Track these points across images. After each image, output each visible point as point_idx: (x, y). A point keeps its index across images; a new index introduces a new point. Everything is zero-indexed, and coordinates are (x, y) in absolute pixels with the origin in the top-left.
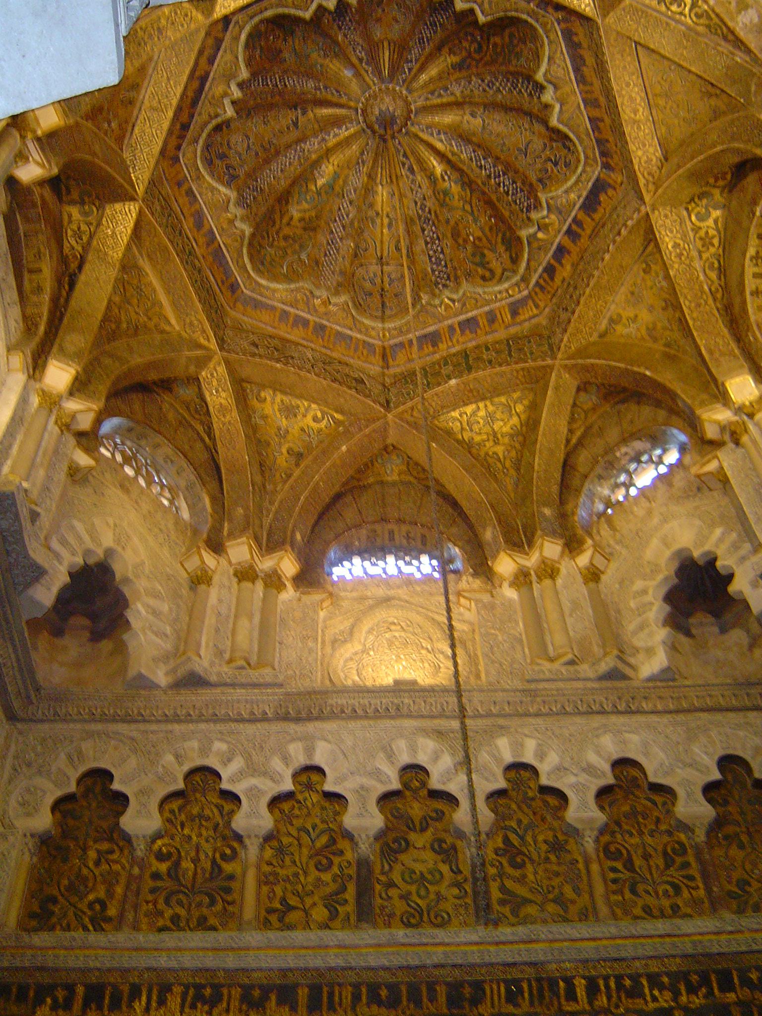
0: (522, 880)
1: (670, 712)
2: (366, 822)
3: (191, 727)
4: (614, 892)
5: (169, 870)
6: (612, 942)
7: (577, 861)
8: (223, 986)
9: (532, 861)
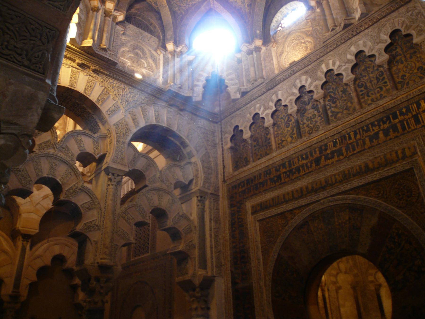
0: (336, 107)
1: (371, 26)
2: (293, 110)
3: (251, 104)
4: (362, 98)
5: (257, 143)
6: (359, 117)
7: (350, 93)
9: (338, 99)
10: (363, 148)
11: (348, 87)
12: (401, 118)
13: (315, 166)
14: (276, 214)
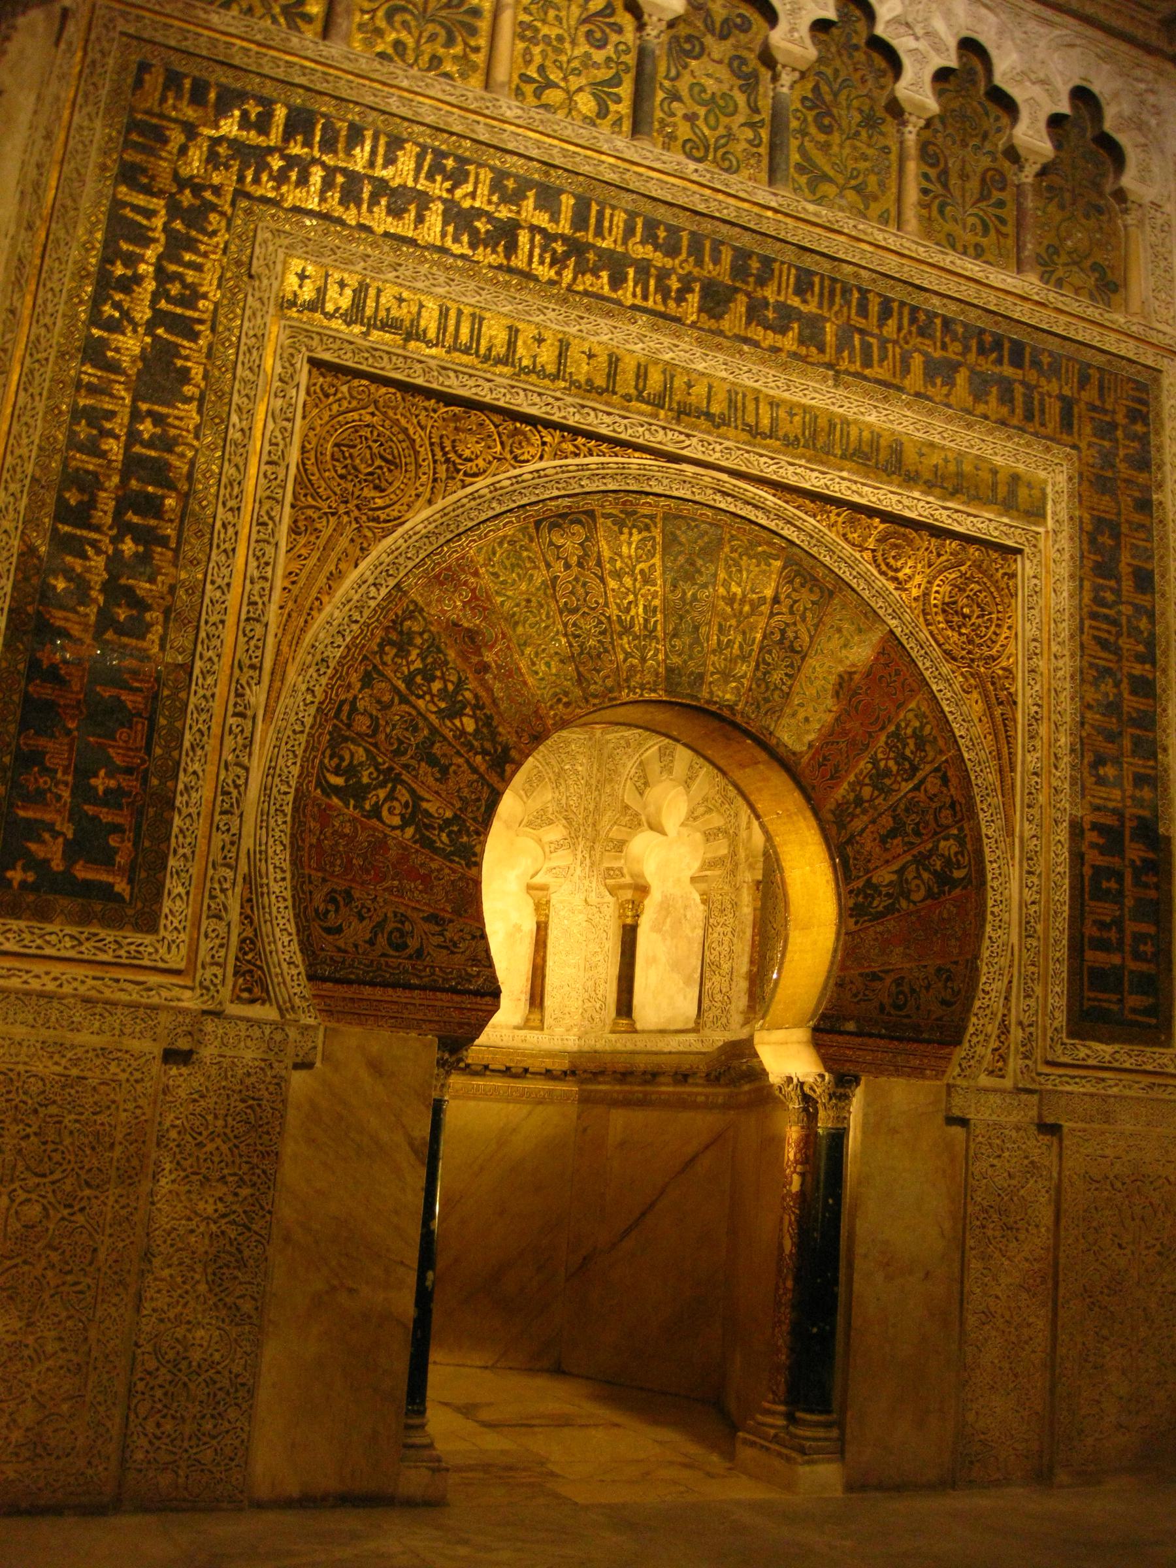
0: (825, 147)
8: (468, 161)
10: (896, 381)
11: (889, 119)
12: (1032, 376)
13: (701, 310)
14: (435, 386)
